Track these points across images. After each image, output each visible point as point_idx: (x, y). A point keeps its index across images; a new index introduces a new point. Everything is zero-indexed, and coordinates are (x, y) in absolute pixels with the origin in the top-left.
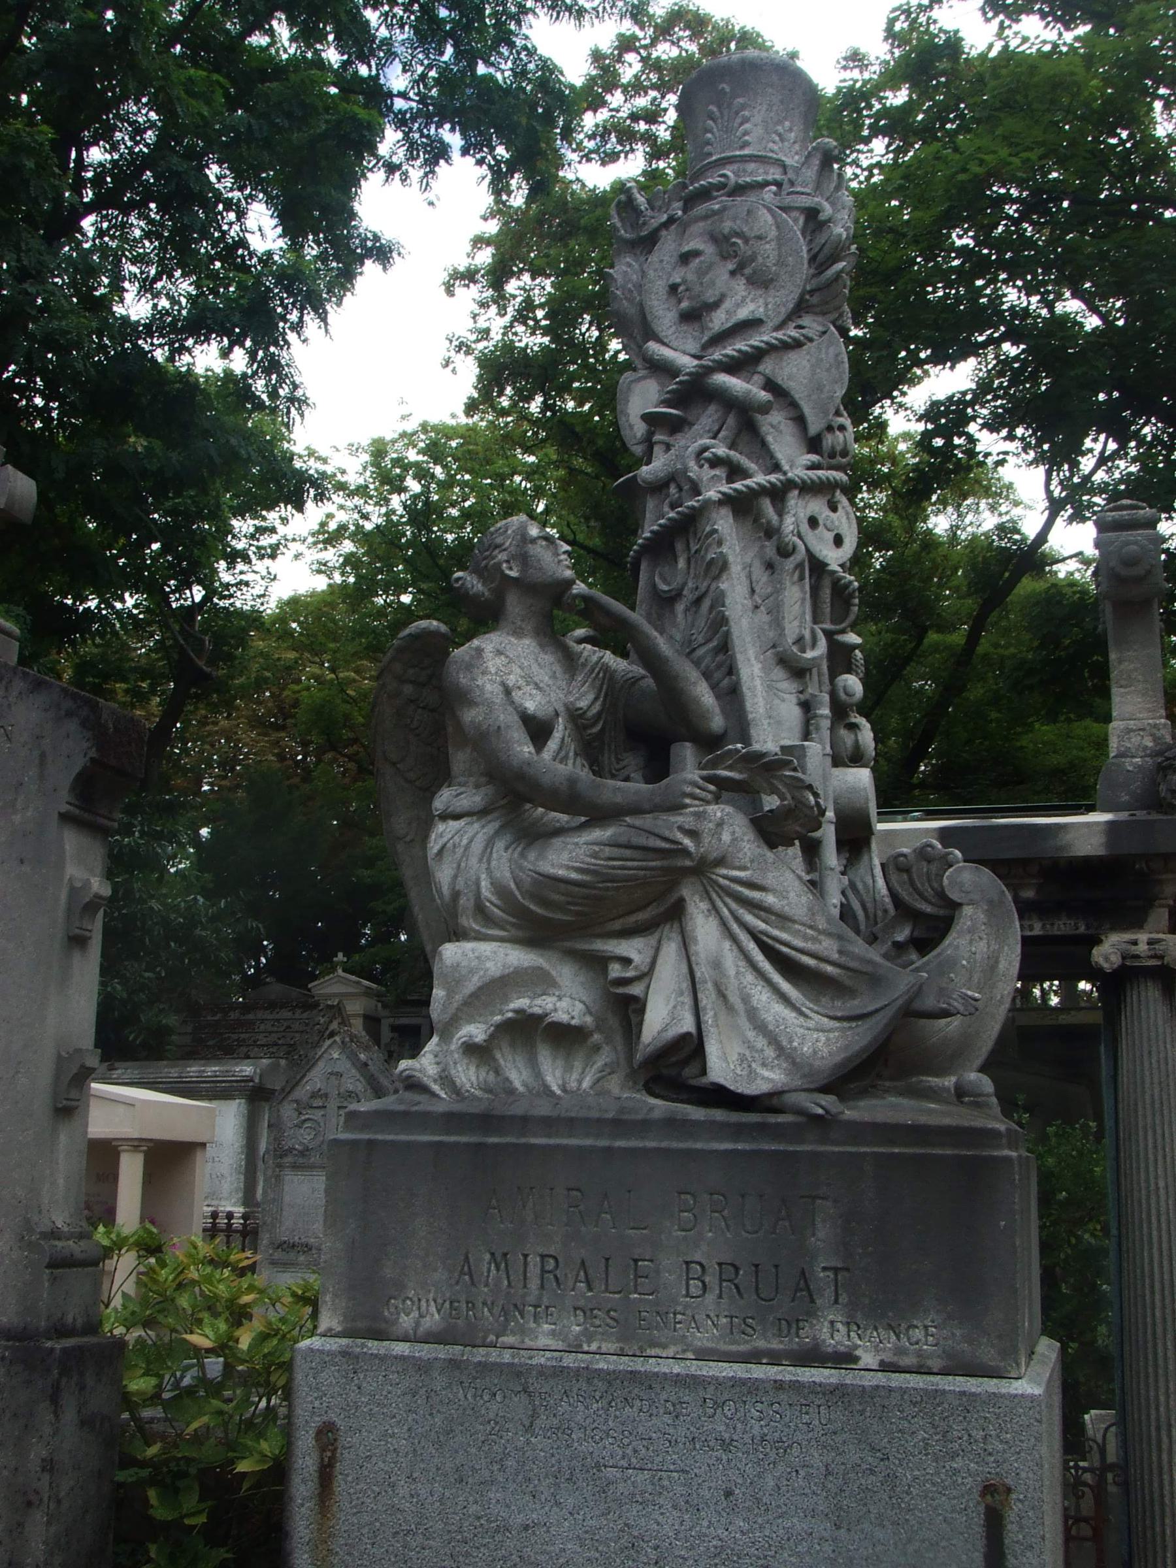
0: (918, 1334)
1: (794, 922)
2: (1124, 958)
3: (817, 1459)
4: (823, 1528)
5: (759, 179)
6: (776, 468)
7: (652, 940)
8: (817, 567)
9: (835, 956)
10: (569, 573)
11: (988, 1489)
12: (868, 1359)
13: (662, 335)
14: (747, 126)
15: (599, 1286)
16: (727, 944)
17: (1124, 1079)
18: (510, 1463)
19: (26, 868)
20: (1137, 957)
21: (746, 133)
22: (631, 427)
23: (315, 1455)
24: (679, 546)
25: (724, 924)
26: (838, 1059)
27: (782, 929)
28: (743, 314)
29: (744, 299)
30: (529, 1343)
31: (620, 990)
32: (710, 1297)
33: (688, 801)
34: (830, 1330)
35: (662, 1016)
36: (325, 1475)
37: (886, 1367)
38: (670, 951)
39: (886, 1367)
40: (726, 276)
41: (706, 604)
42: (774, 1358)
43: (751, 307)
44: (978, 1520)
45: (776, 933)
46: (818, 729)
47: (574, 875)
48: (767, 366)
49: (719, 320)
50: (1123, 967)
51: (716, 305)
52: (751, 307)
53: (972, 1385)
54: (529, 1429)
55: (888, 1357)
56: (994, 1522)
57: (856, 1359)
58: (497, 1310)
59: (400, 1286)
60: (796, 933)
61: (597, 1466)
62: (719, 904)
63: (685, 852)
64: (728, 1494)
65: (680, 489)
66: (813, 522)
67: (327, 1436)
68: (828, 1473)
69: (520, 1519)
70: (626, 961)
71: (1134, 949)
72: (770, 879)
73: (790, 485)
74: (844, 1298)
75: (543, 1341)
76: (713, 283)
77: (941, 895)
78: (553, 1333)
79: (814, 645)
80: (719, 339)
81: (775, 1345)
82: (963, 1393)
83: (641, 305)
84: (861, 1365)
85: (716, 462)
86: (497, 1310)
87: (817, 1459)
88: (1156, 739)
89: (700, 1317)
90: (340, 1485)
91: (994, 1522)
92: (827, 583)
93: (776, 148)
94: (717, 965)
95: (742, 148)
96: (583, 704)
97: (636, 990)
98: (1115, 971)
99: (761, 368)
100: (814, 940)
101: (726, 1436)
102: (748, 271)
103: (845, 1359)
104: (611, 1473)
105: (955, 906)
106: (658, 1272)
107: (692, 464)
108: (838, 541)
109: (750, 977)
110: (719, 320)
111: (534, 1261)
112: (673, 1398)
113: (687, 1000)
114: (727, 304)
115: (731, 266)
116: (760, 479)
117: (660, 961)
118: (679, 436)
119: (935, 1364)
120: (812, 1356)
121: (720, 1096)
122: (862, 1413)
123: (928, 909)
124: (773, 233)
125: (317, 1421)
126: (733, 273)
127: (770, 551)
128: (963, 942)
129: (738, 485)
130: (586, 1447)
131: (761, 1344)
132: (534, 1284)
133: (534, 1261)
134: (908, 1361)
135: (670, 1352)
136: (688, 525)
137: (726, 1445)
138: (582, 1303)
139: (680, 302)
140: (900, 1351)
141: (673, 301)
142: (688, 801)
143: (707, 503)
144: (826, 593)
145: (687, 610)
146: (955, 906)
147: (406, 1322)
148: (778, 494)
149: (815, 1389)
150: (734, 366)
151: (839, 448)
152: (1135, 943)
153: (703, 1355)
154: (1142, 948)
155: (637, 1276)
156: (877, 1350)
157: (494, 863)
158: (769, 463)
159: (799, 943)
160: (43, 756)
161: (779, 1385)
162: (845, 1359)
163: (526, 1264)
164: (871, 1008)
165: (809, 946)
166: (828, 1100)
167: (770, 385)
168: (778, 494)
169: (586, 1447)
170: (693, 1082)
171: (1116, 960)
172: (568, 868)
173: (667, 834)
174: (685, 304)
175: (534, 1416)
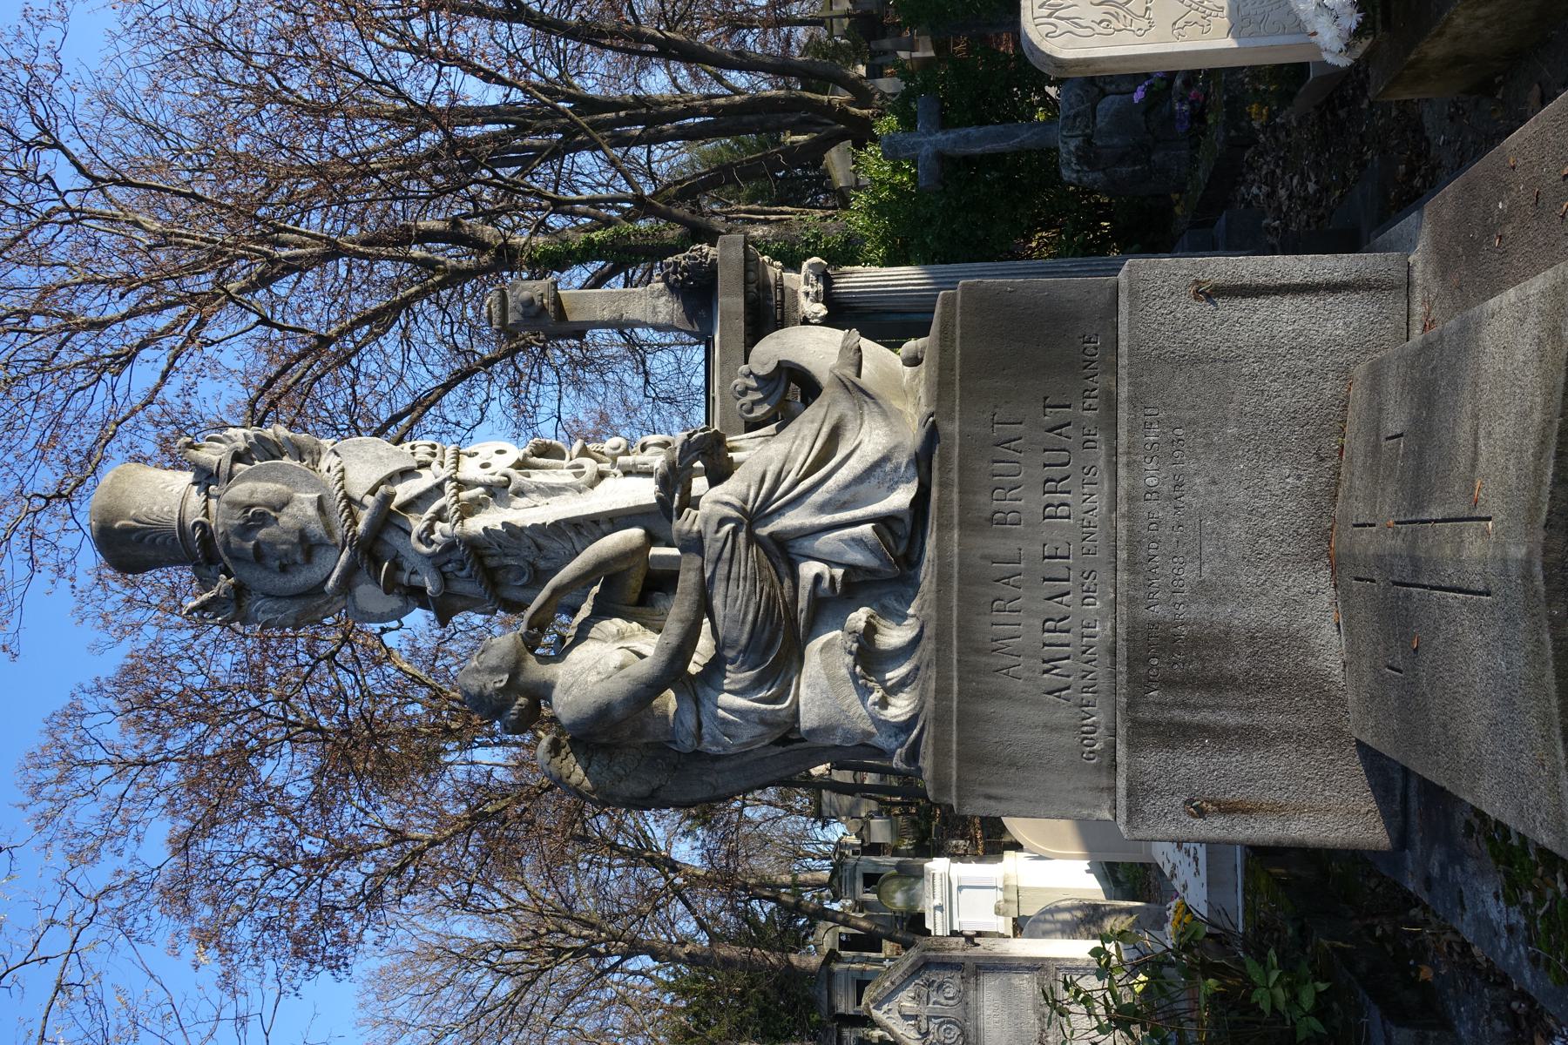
9: (816, 425)
11: (1198, 295)
13: (320, 579)
24: (492, 562)
27: (795, 460)
31: (838, 587)
41: (541, 541)
45: (797, 466)
60: (798, 452)
63: (735, 531)
72: (760, 470)
83: (292, 597)
88: (661, 295)
89: (1087, 506)
94: (823, 508)
98: (828, 308)
109: (831, 483)
118: (406, 564)
121: (920, 502)
131: (1101, 463)
139: (295, 563)
145: (545, 558)
151: (429, 450)
158: (436, 491)
167: (372, 492)
170: (909, 529)
173: (720, 544)
174: (299, 558)
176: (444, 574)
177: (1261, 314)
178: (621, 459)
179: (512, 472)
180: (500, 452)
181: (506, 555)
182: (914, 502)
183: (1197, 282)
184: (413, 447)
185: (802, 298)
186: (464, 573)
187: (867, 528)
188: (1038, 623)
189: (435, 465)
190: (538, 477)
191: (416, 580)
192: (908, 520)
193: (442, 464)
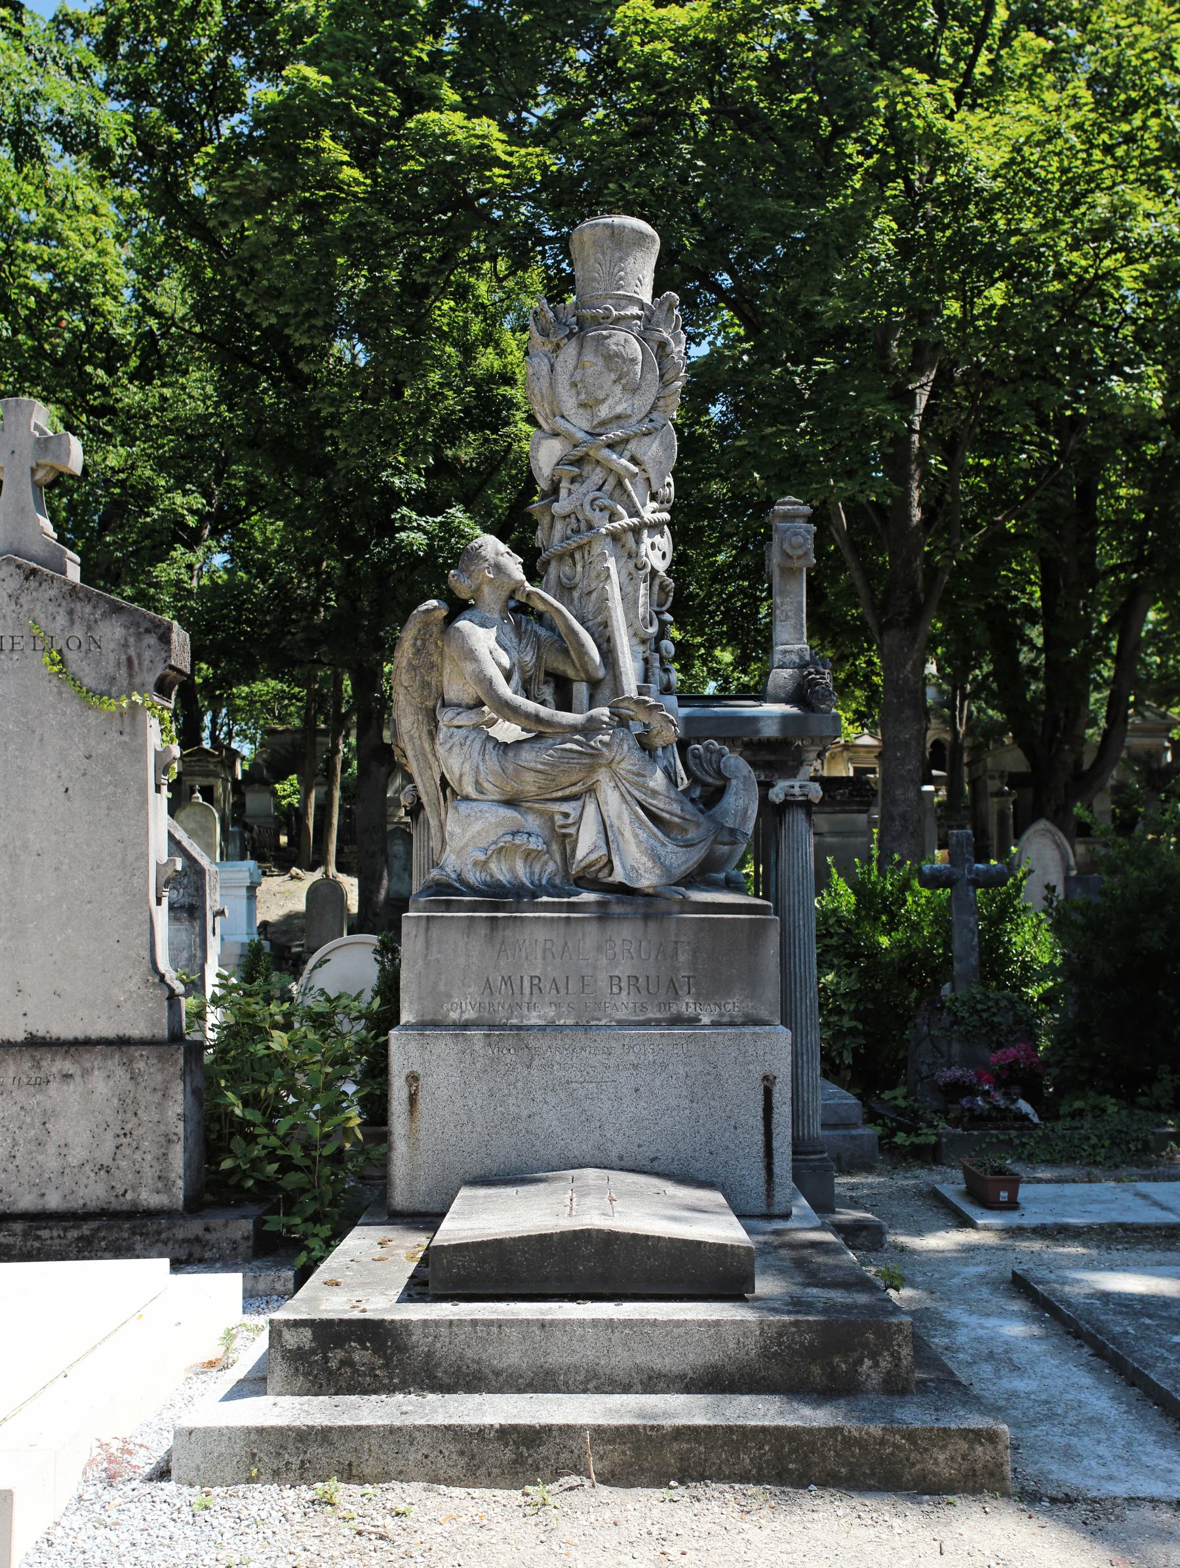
0: (729, 1007)
3: (681, 1071)
4: (685, 1103)
6: (636, 514)
7: (580, 803)
10: (524, 577)
12: (706, 1020)
15: (563, 991)
17: (782, 864)
18: (520, 1084)
19: (126, 738)
23: (406, 1089)
28: (619, 409)
30: (525, 1022)
32: (624, 993)
34: (686, 1006)
35: (587, 844)
36: (413, 1099)
37: (715, 1024)
43: (625, 405)
47: (540, 767)
48: (632, 446)
51: (603, 401)
52: (625, 405)
54: (529, 1067)
55: (715, 1018)
59: (449, 996)
61: (568, 1082)
64: (637, 1090)
66: (653, 546)
67: (413, 1078)
69: (525, 1113)
70: (566, 815)
73: (644, 525)
74: (693, 990)
75: (533, 1021)
77: (719, 773)
78: (539, 1017)
80: (603, 423)
81: (658, 1016)
90: (421, 1105)
92: (657, 582)
96: (528, 659)
97: (572, 830)
103: (693, 1021)
104: (574, 1085)
107: (587, 507)
110: (604, 412)
113: (602, 836)
114: (610, 401)
115: (613, 377)
116: (627, 521)
119: (739, 1020)
120: (677, 1021)
123: (710, 780)
124: (640, 358)
125: (406, 1071)
127: (631, 565)
129: (616, 524)
131: (651, 1015)
132: (527, 991)
134: (726, 1019)
137: (635, 1067)
139: (578, 394)
140: (721, 1015)
141: (574, 391)
144: (656, 588)
145: (580, 598)
146: (727, 780)
147: (454, 1016)
149: (680, 1036)
150: (610, 446)
154: (797, 791)
159: (661, 806)
160: (130, 660)
161: (663, 1035)
162: (693, 1021)
165: (667, 807)
168: (636, 531)
169: (563, 1073)
171: (782, 797)
175: (532, 1059)
177: (751, 1121)
178: (657, 656)
184: (669, 485)
185: (788, 783)
189: (655, 505)
190: (643, 589)
191: (563, 493)
192: (611, 879)
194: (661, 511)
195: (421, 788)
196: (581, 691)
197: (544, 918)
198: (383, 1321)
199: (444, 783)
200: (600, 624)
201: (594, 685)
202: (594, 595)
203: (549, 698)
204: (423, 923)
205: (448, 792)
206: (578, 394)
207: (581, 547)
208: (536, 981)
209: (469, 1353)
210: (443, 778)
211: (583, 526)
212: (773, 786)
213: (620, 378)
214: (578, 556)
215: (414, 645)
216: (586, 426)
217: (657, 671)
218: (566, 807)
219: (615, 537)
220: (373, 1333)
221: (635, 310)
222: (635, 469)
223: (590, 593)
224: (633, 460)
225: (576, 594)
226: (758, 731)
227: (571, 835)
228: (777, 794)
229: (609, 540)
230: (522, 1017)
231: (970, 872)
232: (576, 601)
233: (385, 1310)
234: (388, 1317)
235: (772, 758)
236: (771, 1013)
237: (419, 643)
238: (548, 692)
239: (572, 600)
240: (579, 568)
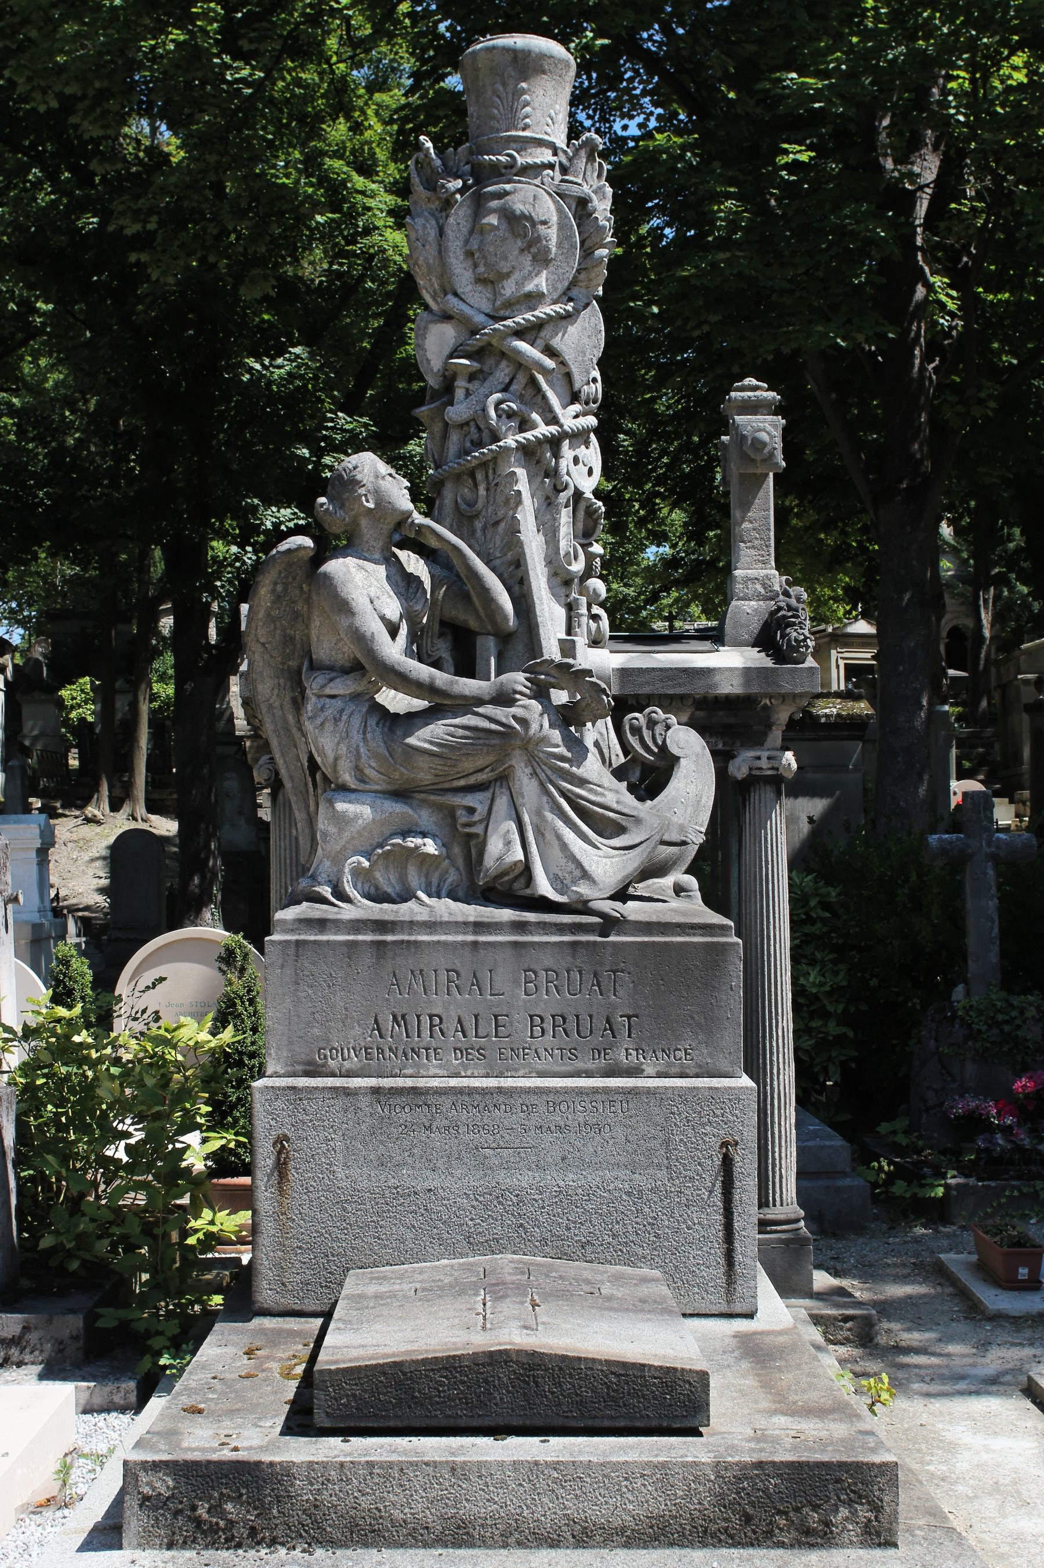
1: (590, 783)
2: (751, 769)
5: (538, 161)
7: (488, 794)
8: (578, 495)
11: (725, 1144)
12: (649, 1070)
13: (459, 291)
14: (528, 109)
16: (545, 799)
17: (746, 857)
20: (761, 769)
21: (527, 117)
22: (428, 361)
25: (542, 785)
26: (619, 877)
29: (530, 272)
31: (467, 830)
33: (518, 696)
38: (502, 803)
39: (660, 1075)
40: (517, 252)
42: (589, 1074)
44: (718, 1161)
46: (579, 626)
48: (545, 333)
49: (509, 289)
50: (750, 775)
51: (508, 275)
53: (715, 1082)
56: (727, 1162)
57: (643, 1070)
58: (400, 1053)
60: (591, 790)
62: (538, 771)
65: (479, 429)
68: (628, 1141)
70: (471, 811)
71: (758, 764)
73: (564, 435)
75: (432, 1071)
76: (505, 258)
77: (663, 748)
78: (440, 1066)
79: (576, 558)
82: (711, 1088)
84: (645, 1074)
85: (510, 415)
86: (400, 1053)
87: (620, 1133)
91: (727, 1162)
92: (582, 506)
93: (549, 130)
95: (524, 129)
97: (478, 829)
98: (744, 779)
99: (543, 334)
100: (602, 795)
101: (562, 1124)
102: (534, 250)
105: (677, 759)
106: (511, 1023)
108: (590, 472)
110: (509, 289)
111: (426, 1021)
112: (528, 1102)
114: (516, 276)
116: (543, 430)
117: (495, 809)
122: (647, 1104)
124: (554, 219)
126: (522, 250)
128: (682, 785)
129: (528, 435)
130: (467, 1138)
133: (426, 1021)
134: (674, 1070)
135: (521, 1073)
136: (491, 464)
138: (459, 1045)
139: (476, 266)
140: (669, 1065)
142: (518, 696)
143: (507, 449)
144: (581, 514)
145: (484, 529)
148: (554, 443)
150: (520, 333)
152: (759, 758)
153: (542, 1075)
154: (764, 763)
155: (497, 1026)
156: (655, 1065)
157: (369, 736)
163: (419, 1021)
164: (637, 841)
166: (618, 905)
168: (554, 443)
170: (521, 893)
172: (431, 743)
176: (467, 424)
179: (571, 491)
180: (590, 472)
181: (488, 490)
182: (544, 899)
183: (737, 1143)
184: (594, 380)
185: (752, 754)
186: (468, 444)
187: (521, 856)
188: (436, 1011)
189: (577, 408)
190: (565, 516)
191: (459, 394)
192: (528, 891)
193: (576, 417)
194: (585, 414)
195: (280, 761)
196: (488, 648)
197: (445, 944)
198: (260, 1462)
199: (313, 766)
200: (510, 564)
201: (505, 639)
202: (502, 525)
203: (446, 655)
204: (292, 951)
205: (318, 776)
206: (476, 266)
207: (484, 465)
208: (437, 1020)
209: (365, 1502)
210: (311, 759)
211: (486, 435)
212: (733, 757)
213: (529, 246)
214: (480, 476)
215: (273, 591)
216: (486, 307)
217: (584, 620)
218: (469, 800)
219: (528, 452)
220: (245, 1478)
221: (545, 156)
222: (550, 363)
223: (497, 523)
224: (550, 352)
225: (478, 525)
226: (715, 686)
227: (477, 835)
228: (739, 769)
229: (520, 455)
230: (418, 1066)
231: (989, 845)
232: (479, 533)
233: (262, 1449)
234: (267, 1458)
235: (732, 720)
236: (732, 1063)
237: (279, 588)
238: (443, 649)
239: (473, 532)
240: (482, 491)
